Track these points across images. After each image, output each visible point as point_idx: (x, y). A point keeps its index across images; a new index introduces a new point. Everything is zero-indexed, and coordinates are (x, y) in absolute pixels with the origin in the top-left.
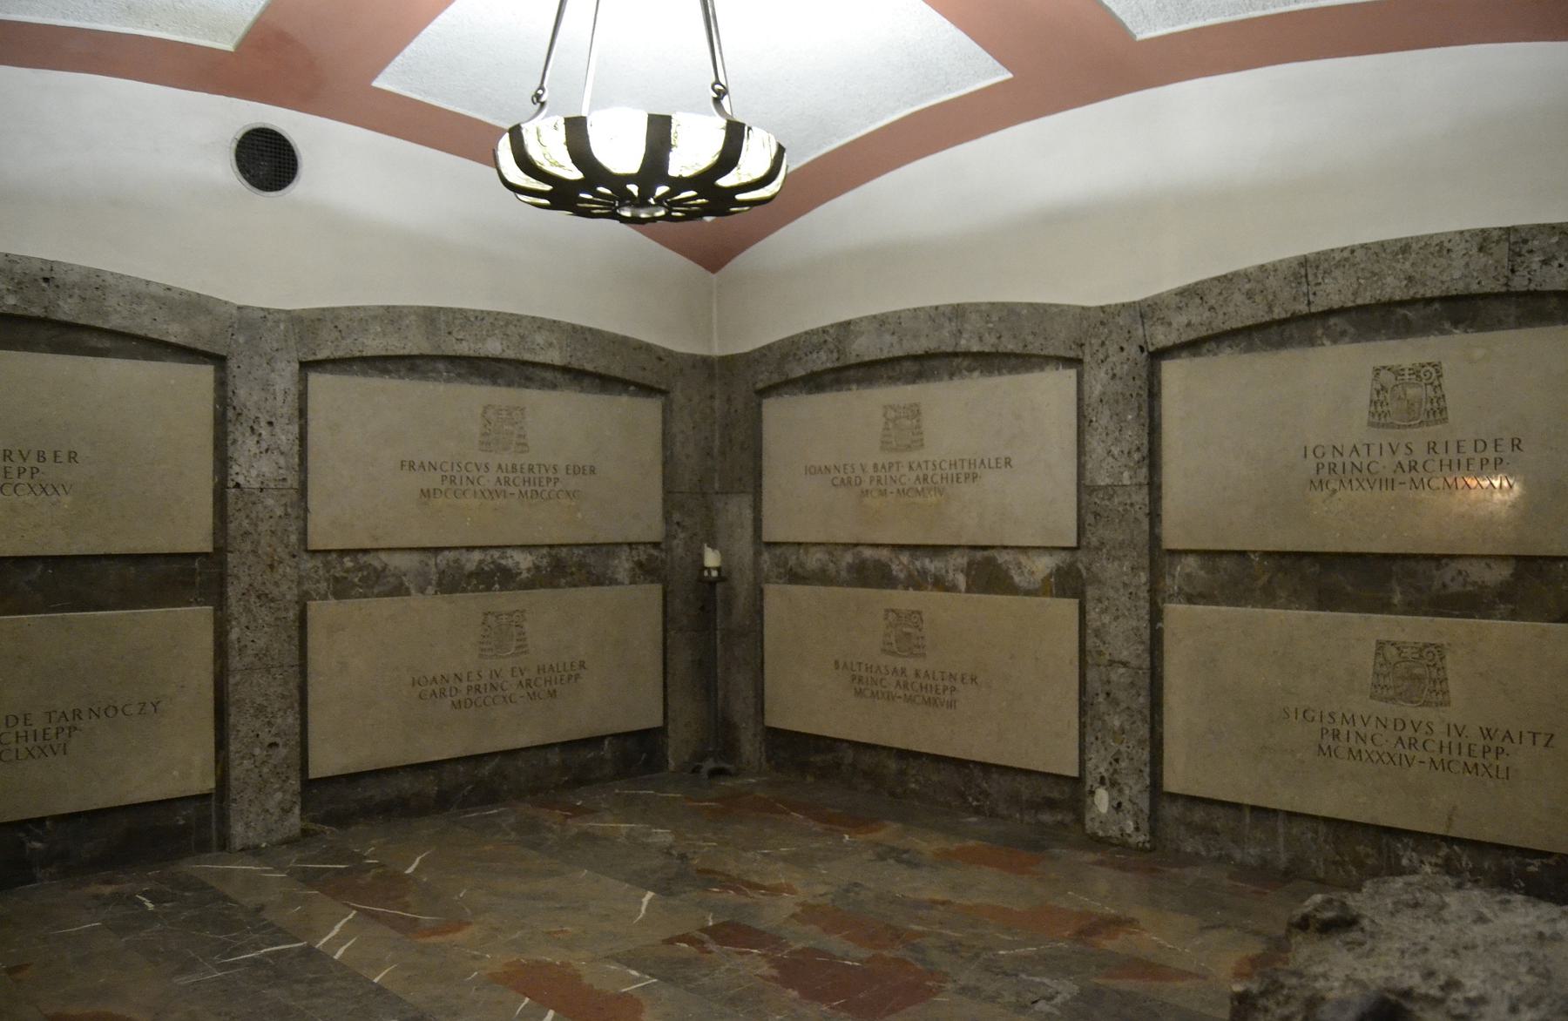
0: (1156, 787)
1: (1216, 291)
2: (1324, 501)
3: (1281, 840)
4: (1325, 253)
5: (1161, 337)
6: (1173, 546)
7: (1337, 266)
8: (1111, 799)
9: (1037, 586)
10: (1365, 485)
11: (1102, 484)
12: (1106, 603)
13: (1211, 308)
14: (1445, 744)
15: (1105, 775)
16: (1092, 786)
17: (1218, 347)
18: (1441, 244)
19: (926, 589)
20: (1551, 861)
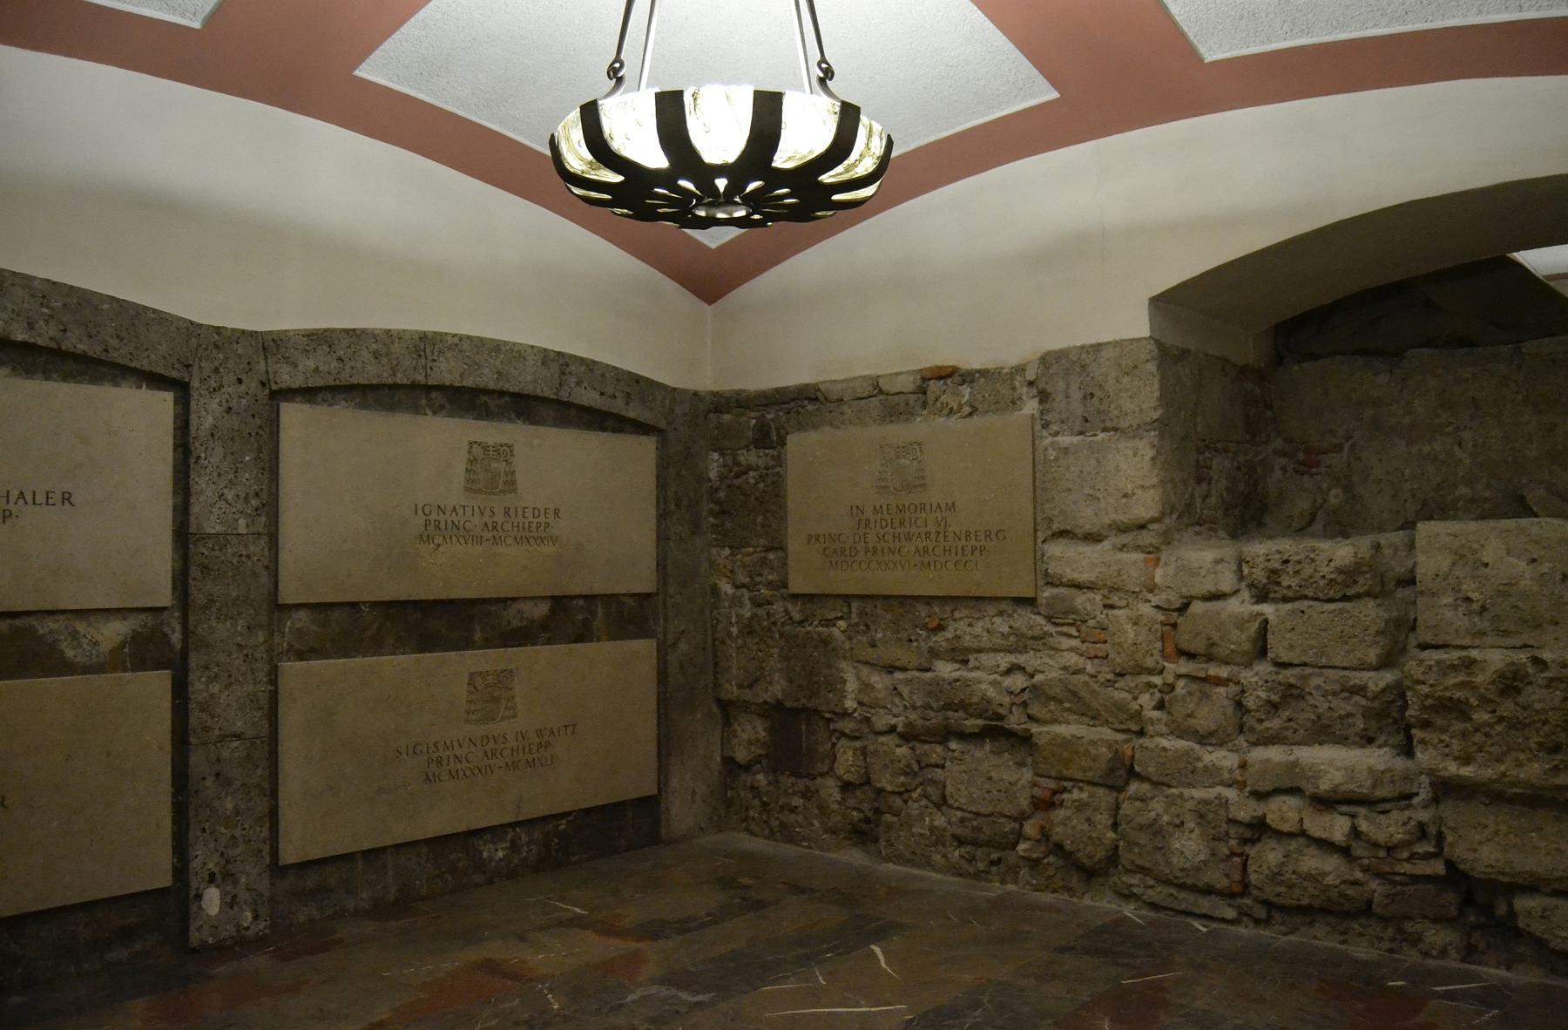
0: (277, 869)
1: (344, 343)
2: (431, 554)
3: (390, 873)
4: (440, 334)
5: (286, 377)
6: (289, 601)
7: (450, 348)
8: (224, 894)
9: (102, 659)
10: (462, 541)
11: (213, 531)
12: (216, 669)
13: (340, 359)
14: (516, 748)
15: (216, 870)
16: (198, 889)
17: (333, 399)
18: (519, 352)
19: (592, 641)
20: (571, 818)
